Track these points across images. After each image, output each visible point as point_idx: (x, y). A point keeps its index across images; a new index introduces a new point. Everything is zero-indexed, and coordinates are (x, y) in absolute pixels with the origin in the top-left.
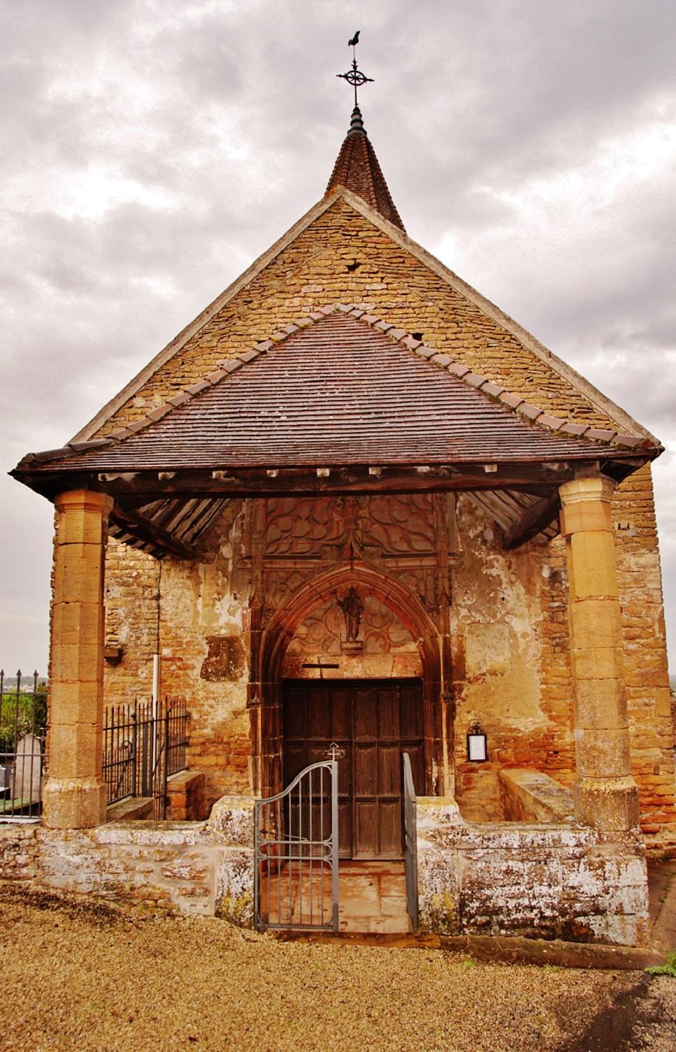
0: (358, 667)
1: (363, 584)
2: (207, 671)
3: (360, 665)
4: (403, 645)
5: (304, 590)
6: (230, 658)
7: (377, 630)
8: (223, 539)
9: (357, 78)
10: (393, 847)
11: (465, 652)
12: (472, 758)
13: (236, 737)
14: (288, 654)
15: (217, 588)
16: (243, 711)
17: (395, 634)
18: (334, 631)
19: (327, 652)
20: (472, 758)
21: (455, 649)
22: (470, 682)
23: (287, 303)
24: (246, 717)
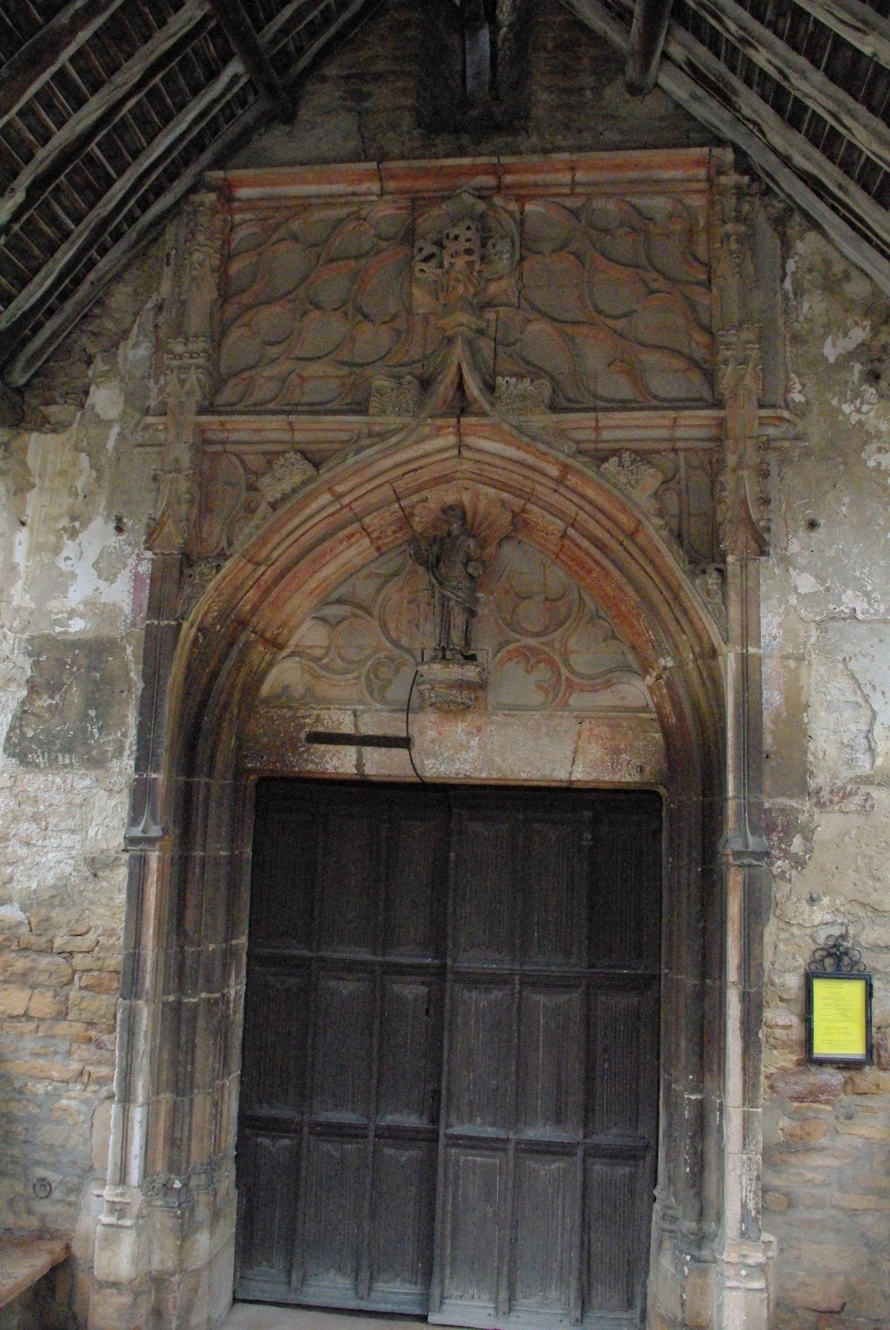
0: (469, 748)
1: (492, 491)
2: (23, 734)
3: (475, 742)
4: (609, 684)
5: (315, 506)
6: (90, 702)
7: (532, 642)
8: (100, 365)
10: (553, 1294)
11: (807, 706)
12: (821, 1048)
13: (92, 937)
14: (267, 701)
15: (71, 500)
16: (116, 859)
17: (585, 653)
18: (404, 641)
19: (384, 701)
20: (821, 1048)
21: (772, 697)
22: (820, 805)
24: (121, 874)
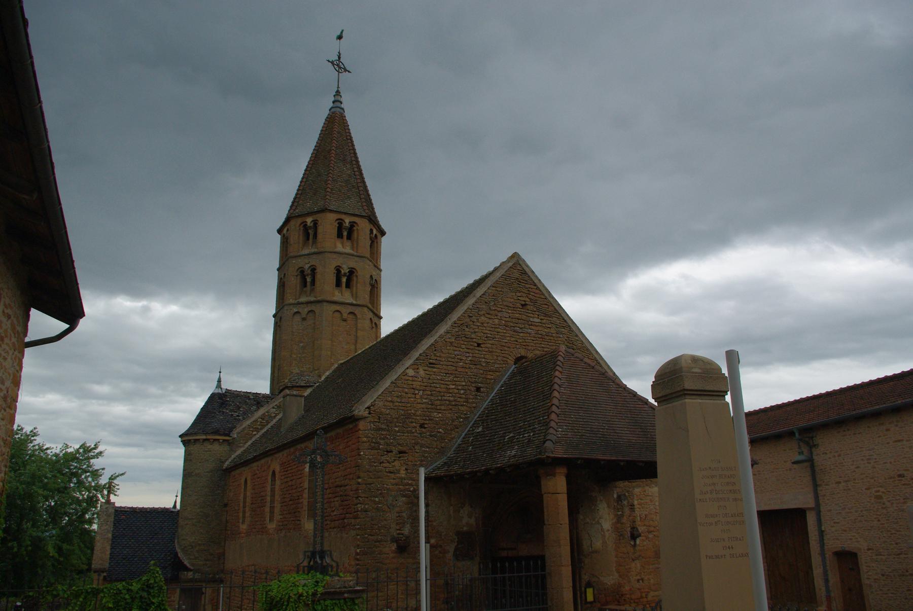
9: (340, 68)
23: (491, 321)
